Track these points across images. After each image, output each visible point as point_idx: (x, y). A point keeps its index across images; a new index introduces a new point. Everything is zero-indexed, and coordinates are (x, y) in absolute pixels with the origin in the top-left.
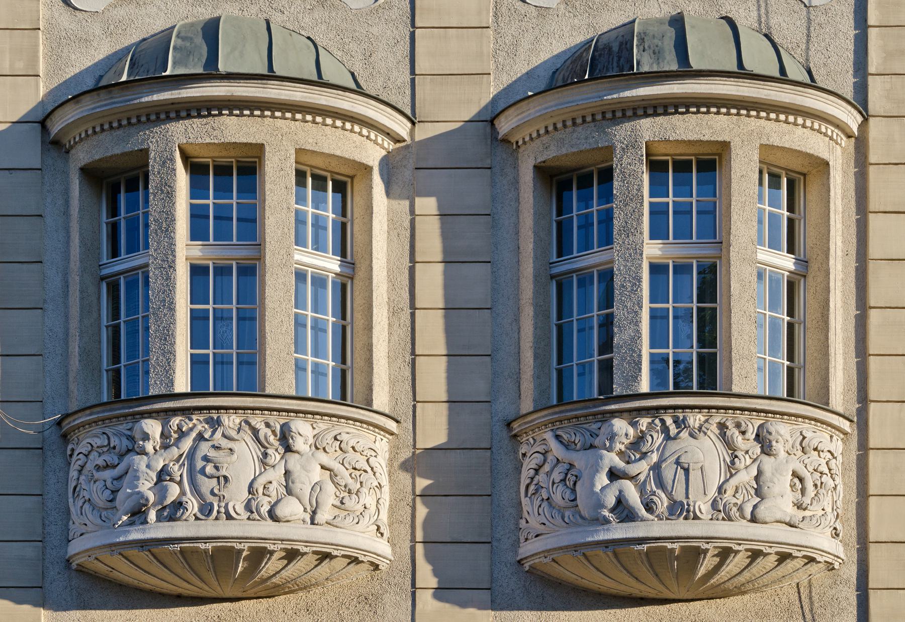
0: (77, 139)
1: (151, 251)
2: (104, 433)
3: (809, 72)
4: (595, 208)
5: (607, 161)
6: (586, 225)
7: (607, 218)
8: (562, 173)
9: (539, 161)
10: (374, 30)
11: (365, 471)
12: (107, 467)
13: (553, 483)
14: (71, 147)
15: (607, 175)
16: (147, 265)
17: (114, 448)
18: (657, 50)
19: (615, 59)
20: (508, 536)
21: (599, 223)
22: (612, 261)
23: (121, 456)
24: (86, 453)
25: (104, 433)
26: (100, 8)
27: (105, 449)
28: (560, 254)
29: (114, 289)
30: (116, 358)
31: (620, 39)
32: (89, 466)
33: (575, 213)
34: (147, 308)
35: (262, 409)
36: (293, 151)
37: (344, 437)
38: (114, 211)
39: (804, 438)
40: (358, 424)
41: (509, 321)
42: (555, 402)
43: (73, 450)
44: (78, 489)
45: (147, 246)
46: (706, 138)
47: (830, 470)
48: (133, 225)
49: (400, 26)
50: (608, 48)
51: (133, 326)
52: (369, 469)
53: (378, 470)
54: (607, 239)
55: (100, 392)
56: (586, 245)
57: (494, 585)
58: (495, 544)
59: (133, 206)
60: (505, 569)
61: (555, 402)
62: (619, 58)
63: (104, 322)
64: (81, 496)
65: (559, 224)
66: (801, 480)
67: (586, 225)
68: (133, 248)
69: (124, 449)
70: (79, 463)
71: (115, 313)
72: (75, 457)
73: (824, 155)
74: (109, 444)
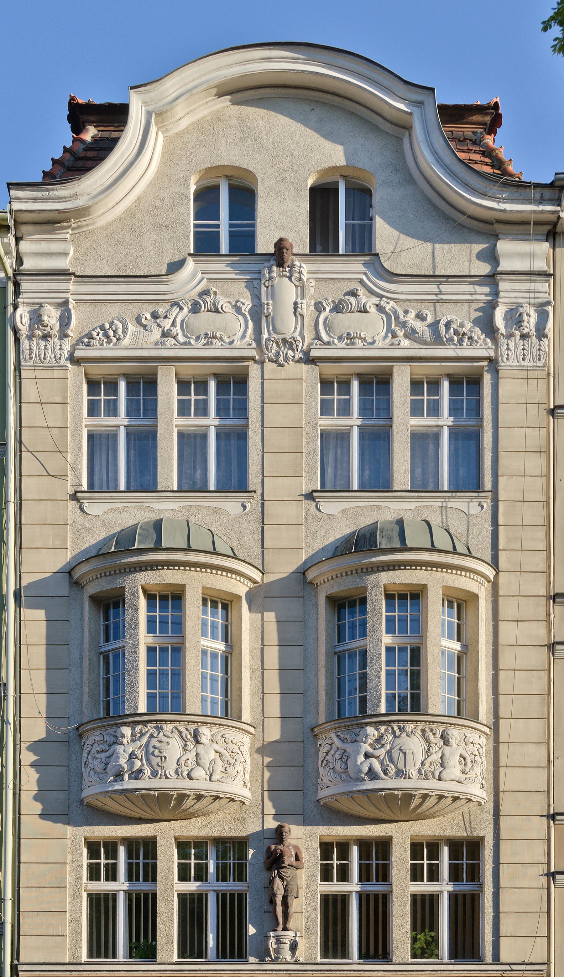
1: (126, 639)
3: (468, 549)
4: (357, 618)
5: (363, 594)
6: (353, 627)
7: (364, 623)
8: (340, 600)
10: (243, 526)
11: (238, 754)
12: (103, 751)
13: (336, 760)
14: (85, 585)
15: (363, 601)
17: (106, 741)
18: (389, 537)
19: (368, 541)
21: (359, 625)
22: (366, 645)
23: (110, 746)
26: (100, 513)
27: (102, 742)
28: (339, 642)
30: (107, 694)
32: (93, 751)
33: (347, 620)
34: (124, 669)
35: (184, 721)
37: (227, 736)
38: (107, 619)
39: (466, 737)
43: (85, 743)
45: (124, 637)
46: (415, 582)
47: (479, 753)
48: (117, 626)
50: (364, 536)
51: (116, 678)
52: (240, 753)
53: (244, 753)
54: (364, 634)
55: (99, 713)
56: (353, 637)
58: (305, 791)
59: (117, 616)
60: (311, 804)
63: (102, 676)
65: (339, 626)
66: (464, 759)
68: (117, 637)
69: (112, 742)
70: (88, 749)
71: (107, 671)
73: (476, 591)
74: (104, 739)
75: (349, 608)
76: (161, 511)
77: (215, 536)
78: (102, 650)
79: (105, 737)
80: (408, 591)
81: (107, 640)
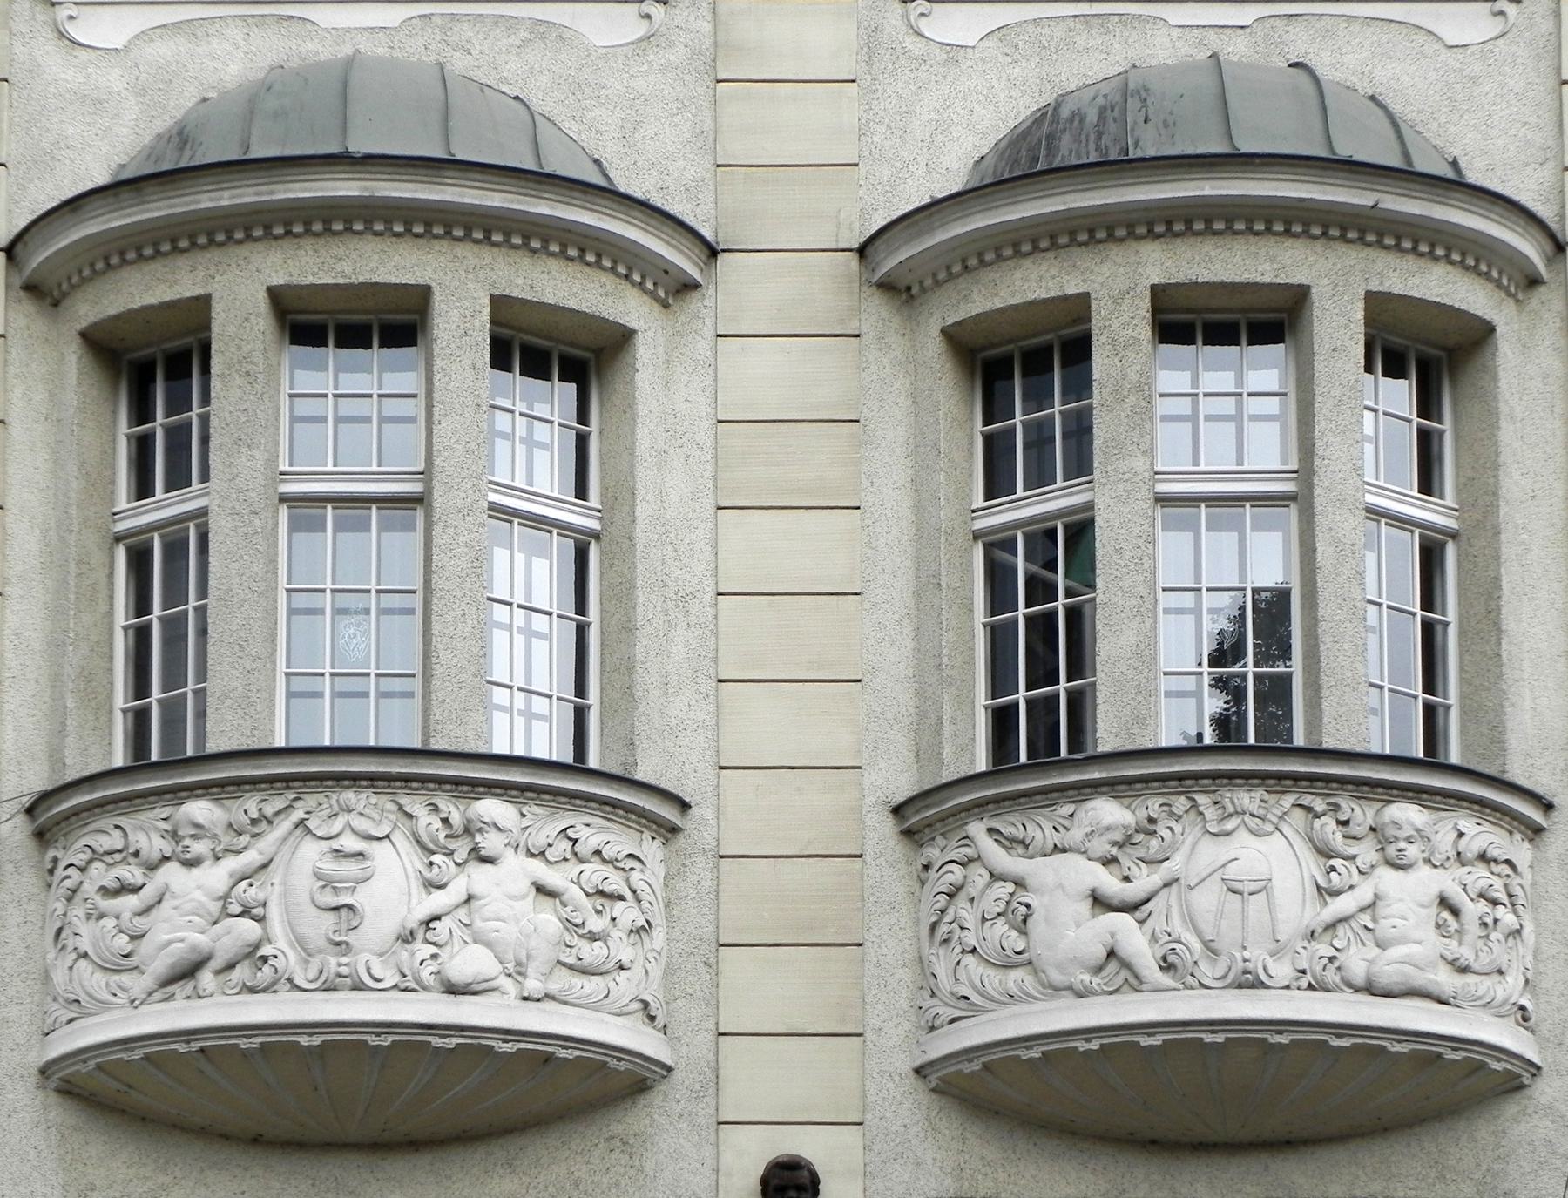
0: (75, 280)
1: (215, 482)
2: (117, 827)
4: (1058, 407)
5: (1075, 322)
6: (1039, 439)
7: (1080, 429)
8: (993, 346)
9: (950, 322)
10: (641, 85)
11: (621, 898)
13: (984, 919)
14: (65, 295)
15: (1078, 350)
16: (203, 512)
17: (136, 854)
18: (1170, 120)
19: (1092, 137)
20: (895, 1021)
21: (1065, 436)
23: (152, 867)
24: (83, 864)
25: (117, 827)
27: (118, 857)
28: (989, 495)
29: (139, 561)
30: (140, 686)
31: (1100, 101)
32: (89, 889)
33: (1019, 417)
35: (424, 780)
36: (487, 301)
37: (581, 833)
38: (142, 413)
39: (1461, 835)
40: (608, 808)
41: (896, 617)
42: (982, 765)
43: (55, 860)
44: (63, 935)
45: (205, 477)
46: (1267, 279)
47: (1510, 896)
48: (178, 440)
49: (687, 78)
50: (1078, 116)
51: (174, 630)
52: (628, 894)
53: (646, 896)
54: (1080, 466)
55: (109, 753)
56: (1040, 477)
57: (869, 1116)
58: (870, 1036)
59: (178, 403)
60: (890, 1085)
61: (982, 765)
62: (1100, 135)
64: (70, 948)
65: (989, 440)
66: (1455, 912)
67: (1039, 439)
68: (178, 479)
69: (156, 856)
70: (68, 883)
71: (142, 604)
72: (59, 873)
74: (126, 847)
75: (1024, 375)
76: (340, 33)
77: (540, 120)
78: (121, 526)
79: (131, 837)
80: (1243, 311)
81: (143, 488)
